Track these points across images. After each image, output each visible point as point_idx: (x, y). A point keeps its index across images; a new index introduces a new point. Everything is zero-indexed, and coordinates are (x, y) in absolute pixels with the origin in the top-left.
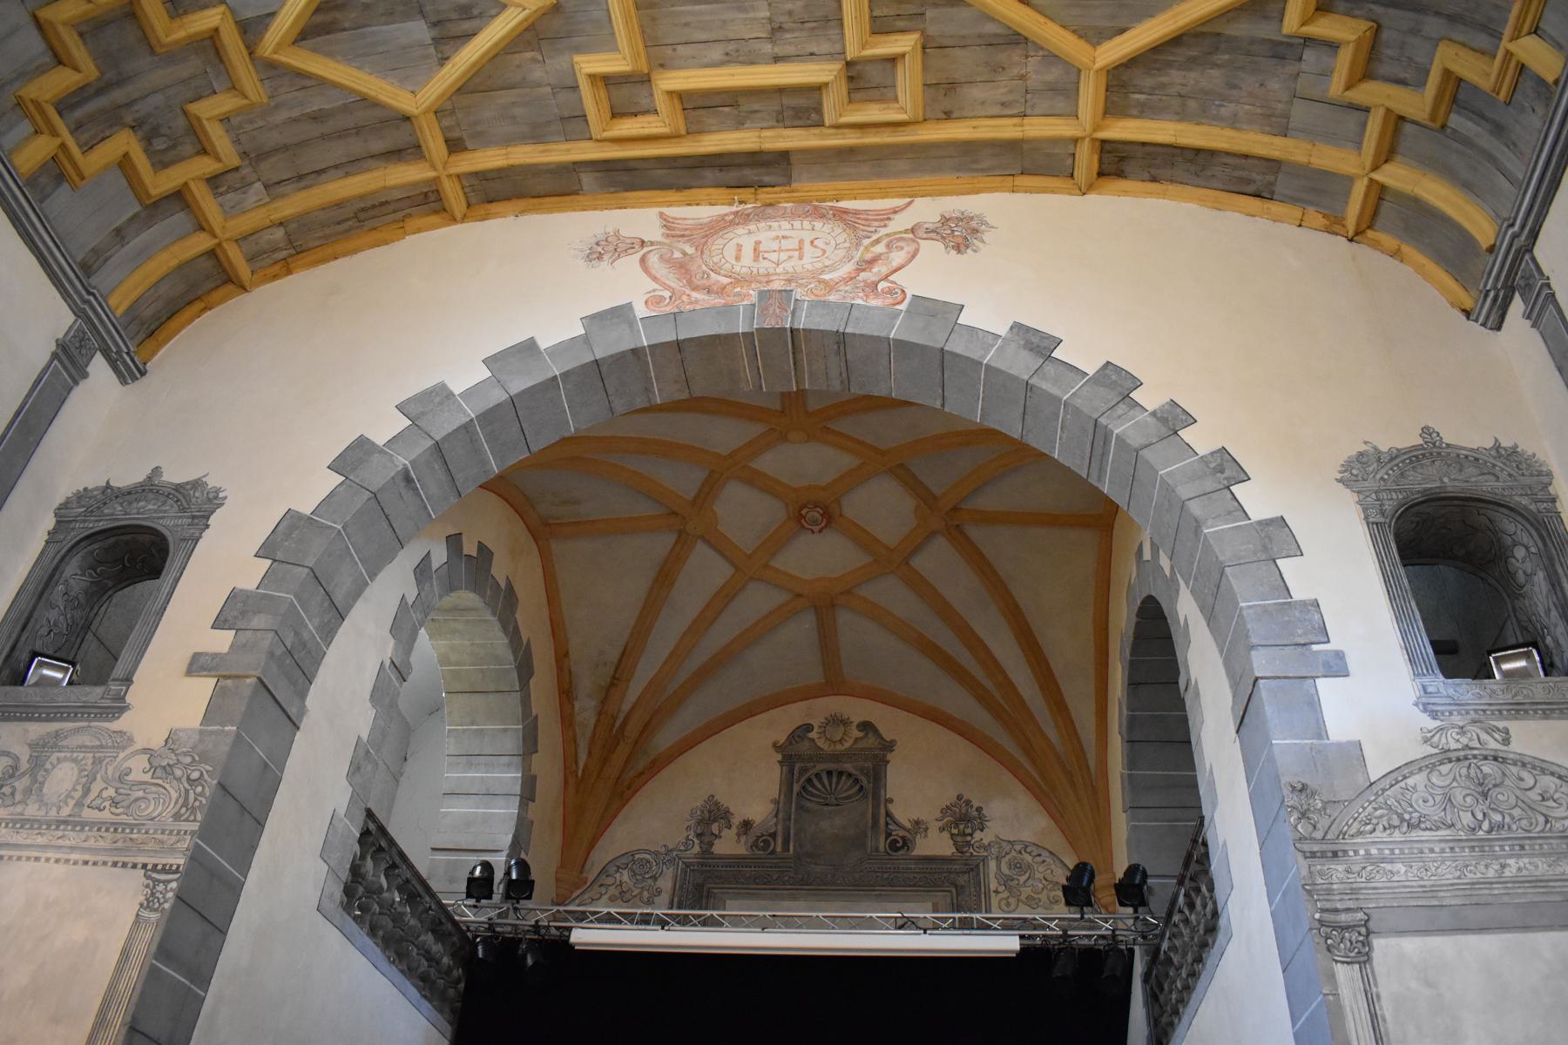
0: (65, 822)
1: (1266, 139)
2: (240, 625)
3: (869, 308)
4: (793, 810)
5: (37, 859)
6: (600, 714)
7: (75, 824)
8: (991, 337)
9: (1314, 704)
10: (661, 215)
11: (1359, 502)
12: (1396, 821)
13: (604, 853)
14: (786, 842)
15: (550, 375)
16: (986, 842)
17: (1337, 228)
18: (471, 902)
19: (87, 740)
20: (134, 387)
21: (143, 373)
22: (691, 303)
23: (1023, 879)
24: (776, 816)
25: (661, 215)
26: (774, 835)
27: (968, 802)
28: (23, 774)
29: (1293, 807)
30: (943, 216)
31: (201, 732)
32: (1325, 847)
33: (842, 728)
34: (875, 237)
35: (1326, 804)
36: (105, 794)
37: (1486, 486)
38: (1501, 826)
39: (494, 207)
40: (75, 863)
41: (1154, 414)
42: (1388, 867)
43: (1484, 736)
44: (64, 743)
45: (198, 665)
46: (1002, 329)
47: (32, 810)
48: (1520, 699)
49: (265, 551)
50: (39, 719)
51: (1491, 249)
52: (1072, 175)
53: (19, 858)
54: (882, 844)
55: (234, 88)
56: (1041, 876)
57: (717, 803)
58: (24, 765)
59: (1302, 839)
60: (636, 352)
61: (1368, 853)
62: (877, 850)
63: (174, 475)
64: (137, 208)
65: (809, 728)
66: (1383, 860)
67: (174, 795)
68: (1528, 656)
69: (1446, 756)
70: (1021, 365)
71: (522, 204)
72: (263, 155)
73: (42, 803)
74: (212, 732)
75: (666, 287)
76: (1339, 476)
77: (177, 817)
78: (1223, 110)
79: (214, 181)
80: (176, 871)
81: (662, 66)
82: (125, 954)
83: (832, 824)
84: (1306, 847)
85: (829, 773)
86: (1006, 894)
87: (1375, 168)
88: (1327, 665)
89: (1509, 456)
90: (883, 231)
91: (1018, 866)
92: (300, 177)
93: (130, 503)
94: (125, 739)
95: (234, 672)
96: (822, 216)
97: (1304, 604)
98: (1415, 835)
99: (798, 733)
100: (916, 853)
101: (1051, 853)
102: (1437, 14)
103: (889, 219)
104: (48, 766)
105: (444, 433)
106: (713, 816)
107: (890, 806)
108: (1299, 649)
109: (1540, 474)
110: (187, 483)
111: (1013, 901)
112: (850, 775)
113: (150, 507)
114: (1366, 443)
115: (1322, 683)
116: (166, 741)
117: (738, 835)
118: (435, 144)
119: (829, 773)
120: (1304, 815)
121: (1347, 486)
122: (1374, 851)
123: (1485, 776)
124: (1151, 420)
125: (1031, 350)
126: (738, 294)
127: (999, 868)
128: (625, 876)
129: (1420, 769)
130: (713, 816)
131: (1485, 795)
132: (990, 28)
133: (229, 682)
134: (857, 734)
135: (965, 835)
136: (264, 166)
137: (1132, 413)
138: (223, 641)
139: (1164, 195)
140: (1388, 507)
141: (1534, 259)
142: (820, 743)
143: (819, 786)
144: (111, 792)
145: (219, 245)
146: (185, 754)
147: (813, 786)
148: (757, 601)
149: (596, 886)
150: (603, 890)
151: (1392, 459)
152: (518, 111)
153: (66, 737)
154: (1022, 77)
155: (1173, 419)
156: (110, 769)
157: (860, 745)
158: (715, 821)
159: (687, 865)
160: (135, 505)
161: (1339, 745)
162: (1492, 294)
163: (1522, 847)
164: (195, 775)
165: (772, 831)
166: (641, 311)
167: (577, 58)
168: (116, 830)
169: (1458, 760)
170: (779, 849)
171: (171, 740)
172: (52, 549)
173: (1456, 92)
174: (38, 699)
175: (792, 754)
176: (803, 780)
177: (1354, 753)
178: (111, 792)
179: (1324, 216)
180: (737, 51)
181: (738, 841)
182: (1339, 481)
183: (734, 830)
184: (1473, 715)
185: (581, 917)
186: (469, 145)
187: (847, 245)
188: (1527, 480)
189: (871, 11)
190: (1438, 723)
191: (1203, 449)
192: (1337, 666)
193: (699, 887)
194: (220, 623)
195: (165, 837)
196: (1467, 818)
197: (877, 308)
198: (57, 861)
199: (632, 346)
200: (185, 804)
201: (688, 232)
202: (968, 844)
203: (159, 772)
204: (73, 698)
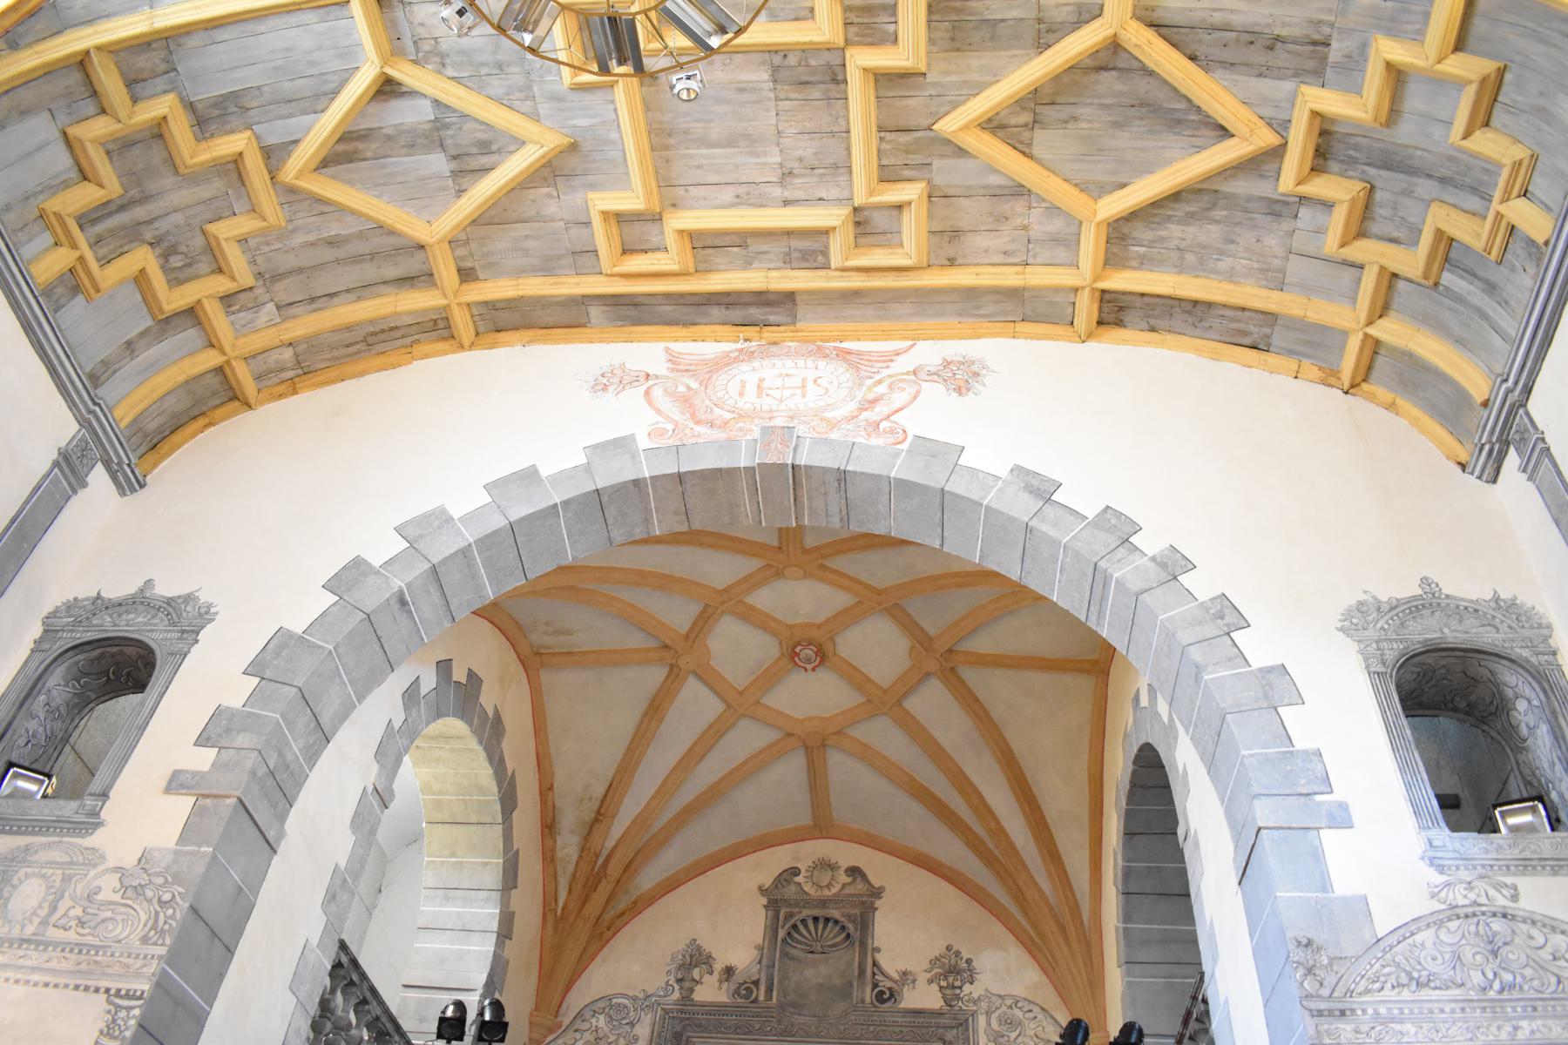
0: (28, 941)
1: (1265, 293)
2: (223, 743)
3: (871, 446)
4: (777, 956)
7: (39, 943)
8: (991, 478)
9: (1318, 856)
10: (667, 349)
11: (1360, 652)
12: (1404, 980)
13: (579, 997)
14: (769, 990)
15: (551, 503)
16: (975, 996)
17: (1332, 380)
19: (57, 855)
20: (130, 498)
21: (142, 486)
22: (693, 436)
23: (1013, 1035)
24: (760, 962)
25: (667, 349)
26: (756, 983)
27: (957, 954)
29: (1299, 963)
30: (944, 360)
31: (176, 852)
32: (1332, 1005)
33: (830, 873)
34: (878, 377)
35: (1332, 960)
36: (72, 913)
37: (1486, 638)
38: (1512, 986)
39: (504, 336)
40: (36, 984)
41: (1153, 559)
42: (1398, 1027)
43: (1492, 892)
44: (34, 858)
45: (176, 783)
46: (1003, 472)
48: (1527, 854)
49: (255, 668)
50: (10, 832)
51: (1485, 404)
52: (1072, 323)
54: (868, 995)
55: (254, 210)
56: (1032, 1033)
57: (699, 948)
59: (1308, 996)
60: (637, 483)
61: (1376, 1012)
62: (863, 1001)
63: (165, 589)
64: (149, 322)
65: (795, 871)
66: (1393, 1020)
67: (144, 917)
68: (1534, 810)
69: (1454, 912)
70: (1021, 507)
71: (530, 333)
72: (277, 277)
74: (186, 853)
75: (667, 418)
76: (1339, 625)
77: (145, 940)
78: (1220, 264)
79: (227, 300)
80: (140, 998)
81: (674, 205)
83: (818, 972)
84: (1314, 1005)
85: (816, 919)
87: (1370, 323)
88: (1331, 816)
89: (1510, 608)
90: (885, 372)
91: (1009, 1022)
92: (313, 300)
93: (120, 616)
94: (95, 857)
95: (214, 792)
96: (825, 357)
97: (1306, 753)
98: (1425, 994)
99: (785, 876)
100: (903, 1005)
101: (1043, 1009)
102: (1429, 176)
103: (892, 360)
104: (15, 881)
105: (441, 557)
106: (695, 960)
107: (879, 957)
108: (1302, 799)
109: (1540, 626)
110: (179, 597)
112: (836, 922)
113: (140, 619)
114: (1365, 592)
115: (1329, 838)
116: (140, 860)
117: (720, 981)
118: (446, 272)
119: (816, 919)
120: (1310, 971)
121: (1348, 635)
122: (1383, 1011)
123: (1495, 934)
124: (1152, 565)
125: (1031, 492)
126: (741, 429)
127: (989, 1024)
128: (601, 1021)
129: (1428, 926)
130: (695, 960)
131: (1495, 953)
132: (994, 180)
133: (208, 801)
134: (844, 879)
135: (954, 987)
136: (279, 286)
137: (1131, 557)
138: (205, 759)
139: (1162, 345)
140: (1390, 656)
141: (1528, 414)
142: (807, 888)
143: (804, 932)
144: (78, 911)
145: (228, 362)
146: (158, 874)
147: (799, 932)
148: (747, 739)
149: (570, 1032)
150: (578, 1035)
151: (1392, 609)
152: (530, 244)
154: (1025, 228)
155: (1173, 566)
156: (78, 890)
157: (847, 891)
158: (696, 966)
160: (124, 616)
161: (1345, 899)
162: (1487, 448)
163: (1535, 1009)
164: (167, 897)
165: (755, 978)
166: (643, 443)
167: (591, 195)
168: (80, 952)
169: (1467, 916)
170: (762, 997)
172: (39, 656)
173: (1447, 250)
174: (11, 811)
175: (778, 898)
176: (787, 927)
177: (1360, 907)
178: (78, 911)
179: (1320, 369)
180: (748, 194)
182: (1341, 629)
183: (716, 975)
184: (1480, 870)
186: (481, 276)
187: (850, 384)
188: (1526, 633)
189: (880, 159)
190: (1444, 878)
191: (1203, 596)
192: (1341, 818)
194: (202, 741)
195: (131, 961)
196: (1477, 978)
197: (875, 447)
198: (17, 982)
199: (634, 477)
200: (154, 927)
201: (692, 368)
202: (957, 997)
203: (130, 893)
204: (46, 811)
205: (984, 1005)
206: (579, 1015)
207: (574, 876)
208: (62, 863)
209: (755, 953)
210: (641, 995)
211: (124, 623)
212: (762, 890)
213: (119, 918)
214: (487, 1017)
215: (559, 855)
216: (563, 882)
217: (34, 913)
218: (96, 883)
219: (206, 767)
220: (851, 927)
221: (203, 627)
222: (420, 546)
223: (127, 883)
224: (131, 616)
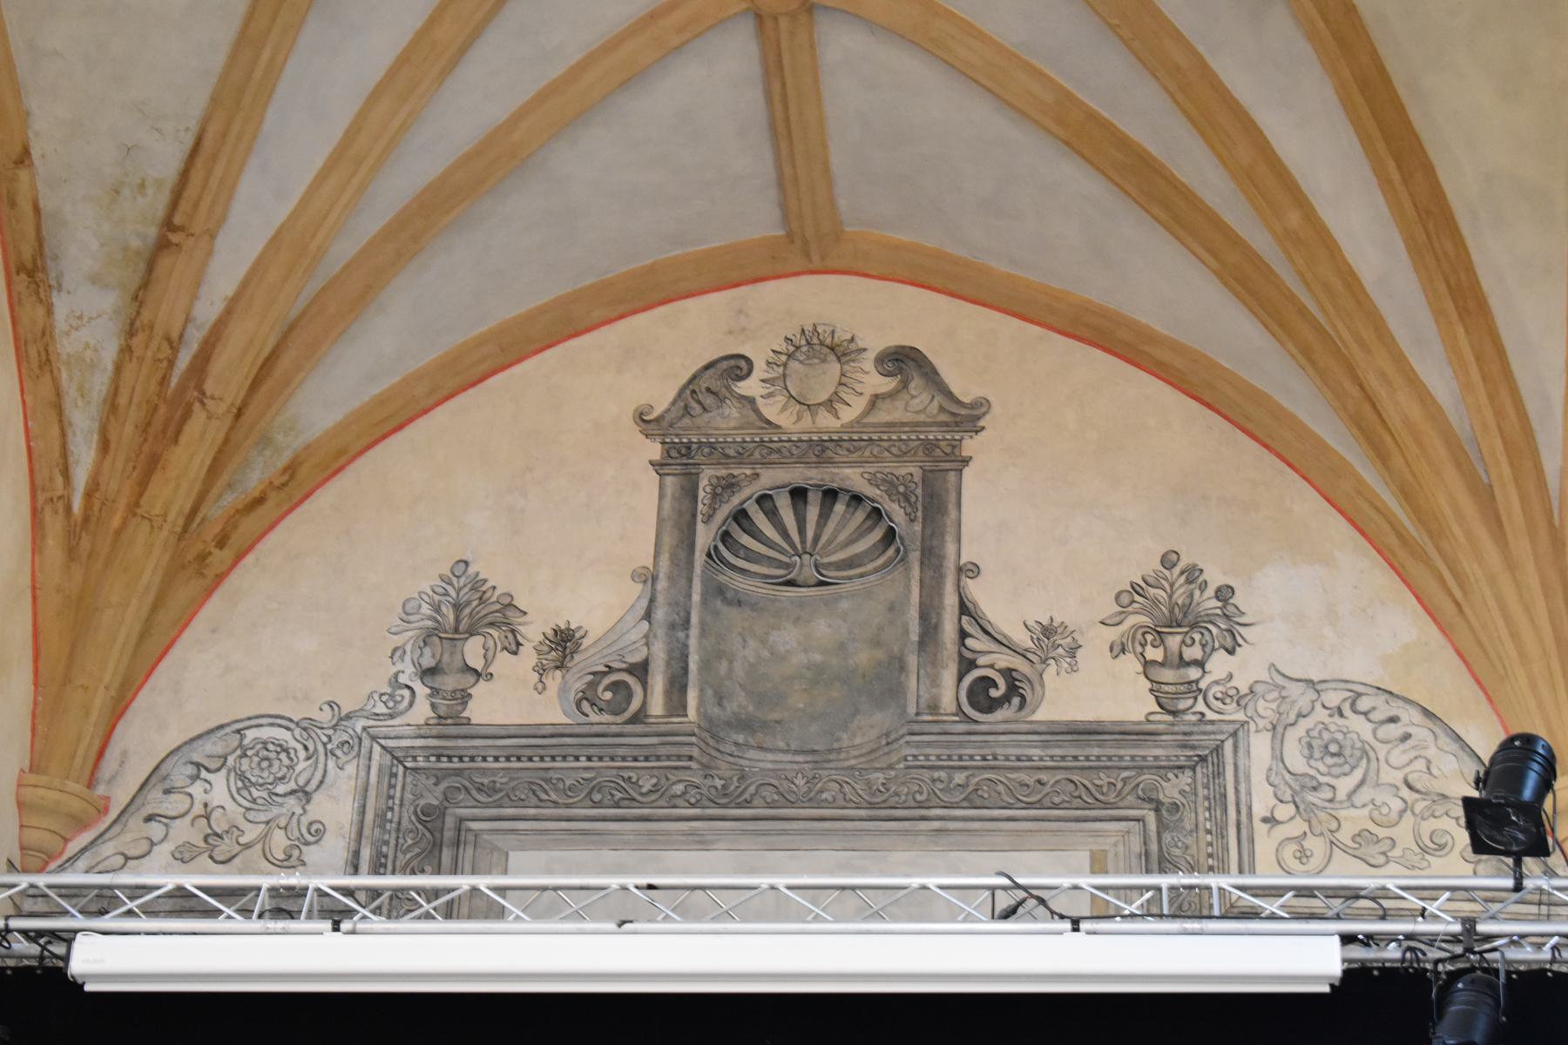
4: (696, 598)
14: (677, 687)
23: (1345, 785)
24: (648, 615)
26: (641, 670)
27: (1192, 574)
33: (834, 368)
54: (949, 691)
56: (1397, 777)
57: (477, 584)
62: (934, 708)
65: (738, 367)
85: (799, 495)
86: (1298, 827)
91: (1334, 751)
100: (1045, 713)
101: (1427, 713)
107: (976, 590)
111: (1316, 845)
112: (857, 499)
117: (541, 670)
128: (219, 789)
134: (880, 383)
135: (1183, 663)
142: (770, 411)
149: (135, 822)
150: (156, 830)
157: (883, 416)
158: (471, 632)
159: (394, 755)
176: (725, 510)
181: (541, 688)
183: (528, 657)
185: (101, 902)
193: (430, 818)
202: (1193, 689)
205: (1265, 708)
207: (112, 405)
209: (634, 592)
210: (326, 717)
212: (645, 421)
215: (67, 346)
216: (83, 422)
220: (896, 512)
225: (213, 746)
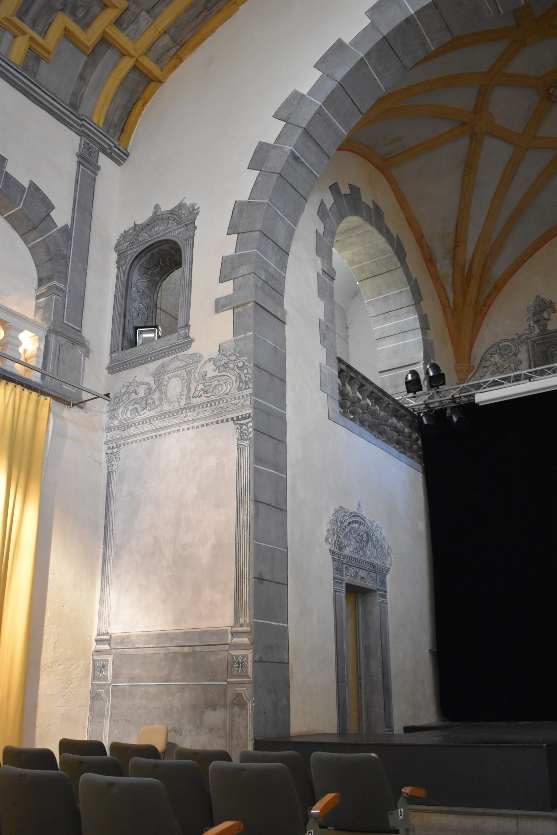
0: (185, 409)
5: (178, 431)
6: (454, 266)
7: (190, 408)
13: (479, 350)
15: (358, 58)
18: (411, 395)
19: (178, 363)
20: (125, 165)
21: (127, 155)
28: (155, 391)
36: (199, 388)
40: (197, 427)
44: (169, 369)
47: (166, 407)
50: (152, 361)
53: (169, 433)
57: (543, 300)
58: (154, 387)
60: (409, 20)
63: (167, 206)
64: (85, 58)
67: (234, 378)
73: (170, 403)
77: (239, 389)
79: (118, 22)
80: (249, 417)
82: (239, 466)
93: (151, 231)
94: (197, 358)
95: (240, 303)
104: (165, 383)
105: (307, 122)
110: (176, 208)
113: (162, 228)
116: (219, 351)
128: (497, 358)
138: (228, 288)
144: (201, 386)
145: (137, 61)
146: (231, 355)
150: (486, 370)
153: (168, 366)
156: (196, 375)
158: (544, 311)
159: (534, 342)
160: (153, 230)
164: (241, 364)
171: (221, 349)
174: (147, 350)
178: (201, 386)
185: (478, 387)
193: (544, 353)
194: (222, 279)
195: (237, 401)
198: (188, 429)
199: (404, 17)
200: (241, 381)
203: (222, 369)
206: (483, 359)
207: (454, 283)
208: (183, 366)
210: (516, 337)
211: (155, 234)
213: (222, 382)
214: (431, 374)
216: (448, 288)
217: (181, 395)
218: (203, 370)
219: (231, 292)
221: (195, 219)
222: (291, 120)
223: (218, 365)
224: (156, 228)
225: (494, 349)
